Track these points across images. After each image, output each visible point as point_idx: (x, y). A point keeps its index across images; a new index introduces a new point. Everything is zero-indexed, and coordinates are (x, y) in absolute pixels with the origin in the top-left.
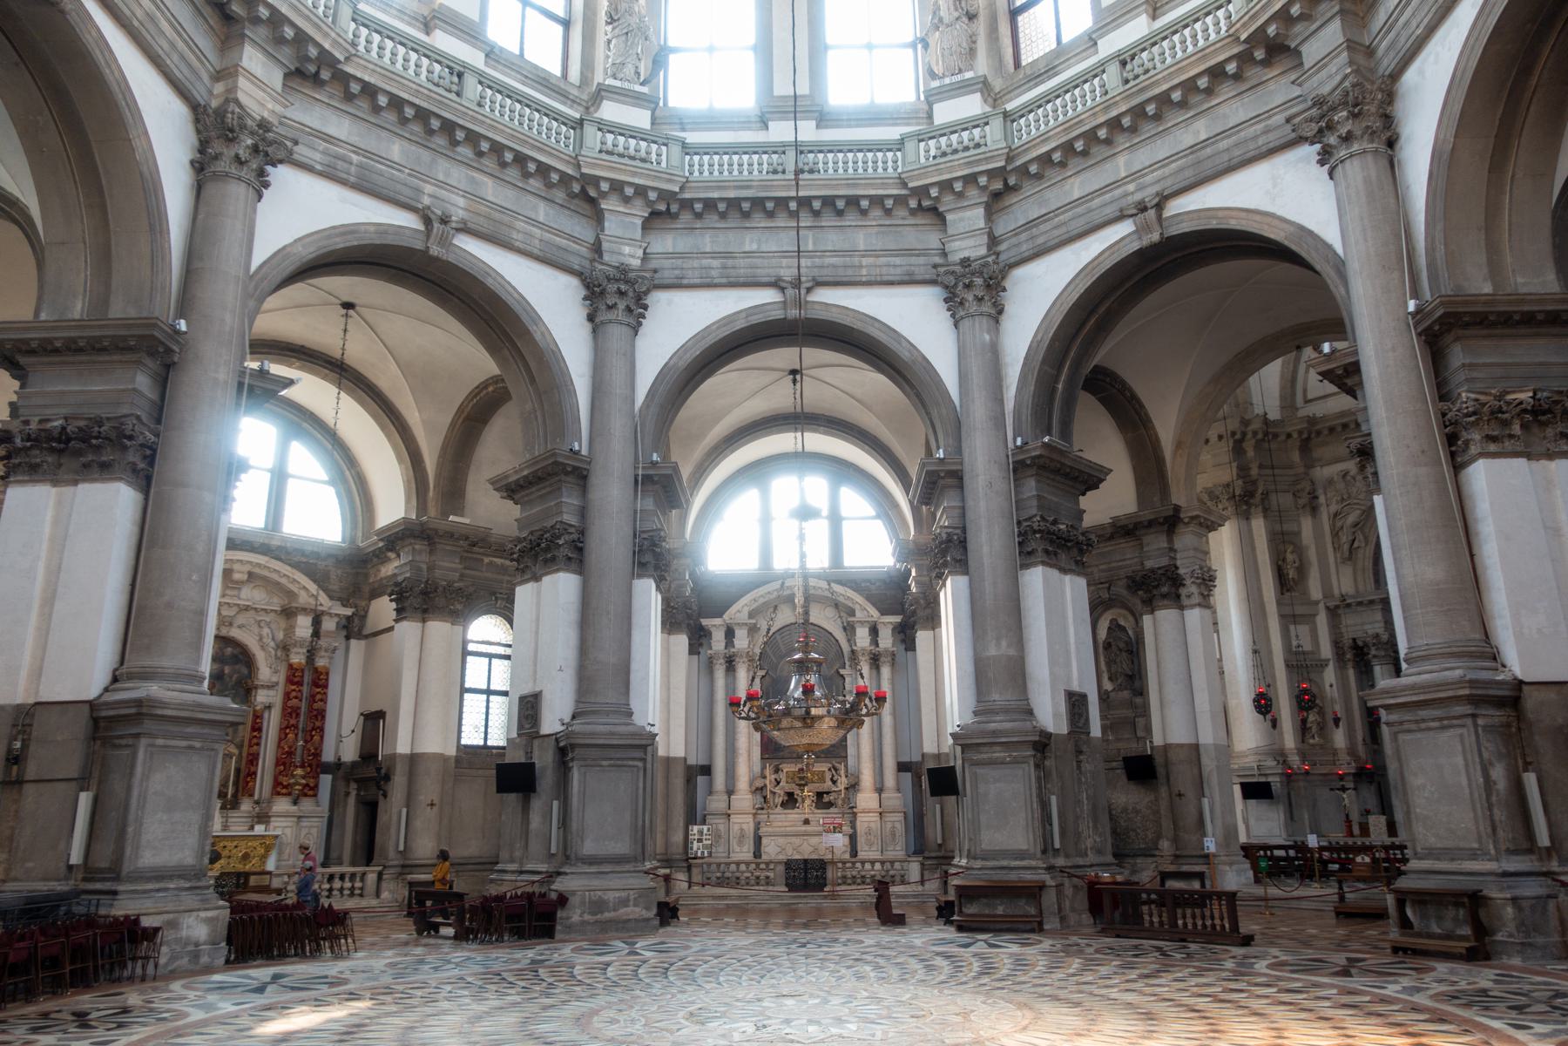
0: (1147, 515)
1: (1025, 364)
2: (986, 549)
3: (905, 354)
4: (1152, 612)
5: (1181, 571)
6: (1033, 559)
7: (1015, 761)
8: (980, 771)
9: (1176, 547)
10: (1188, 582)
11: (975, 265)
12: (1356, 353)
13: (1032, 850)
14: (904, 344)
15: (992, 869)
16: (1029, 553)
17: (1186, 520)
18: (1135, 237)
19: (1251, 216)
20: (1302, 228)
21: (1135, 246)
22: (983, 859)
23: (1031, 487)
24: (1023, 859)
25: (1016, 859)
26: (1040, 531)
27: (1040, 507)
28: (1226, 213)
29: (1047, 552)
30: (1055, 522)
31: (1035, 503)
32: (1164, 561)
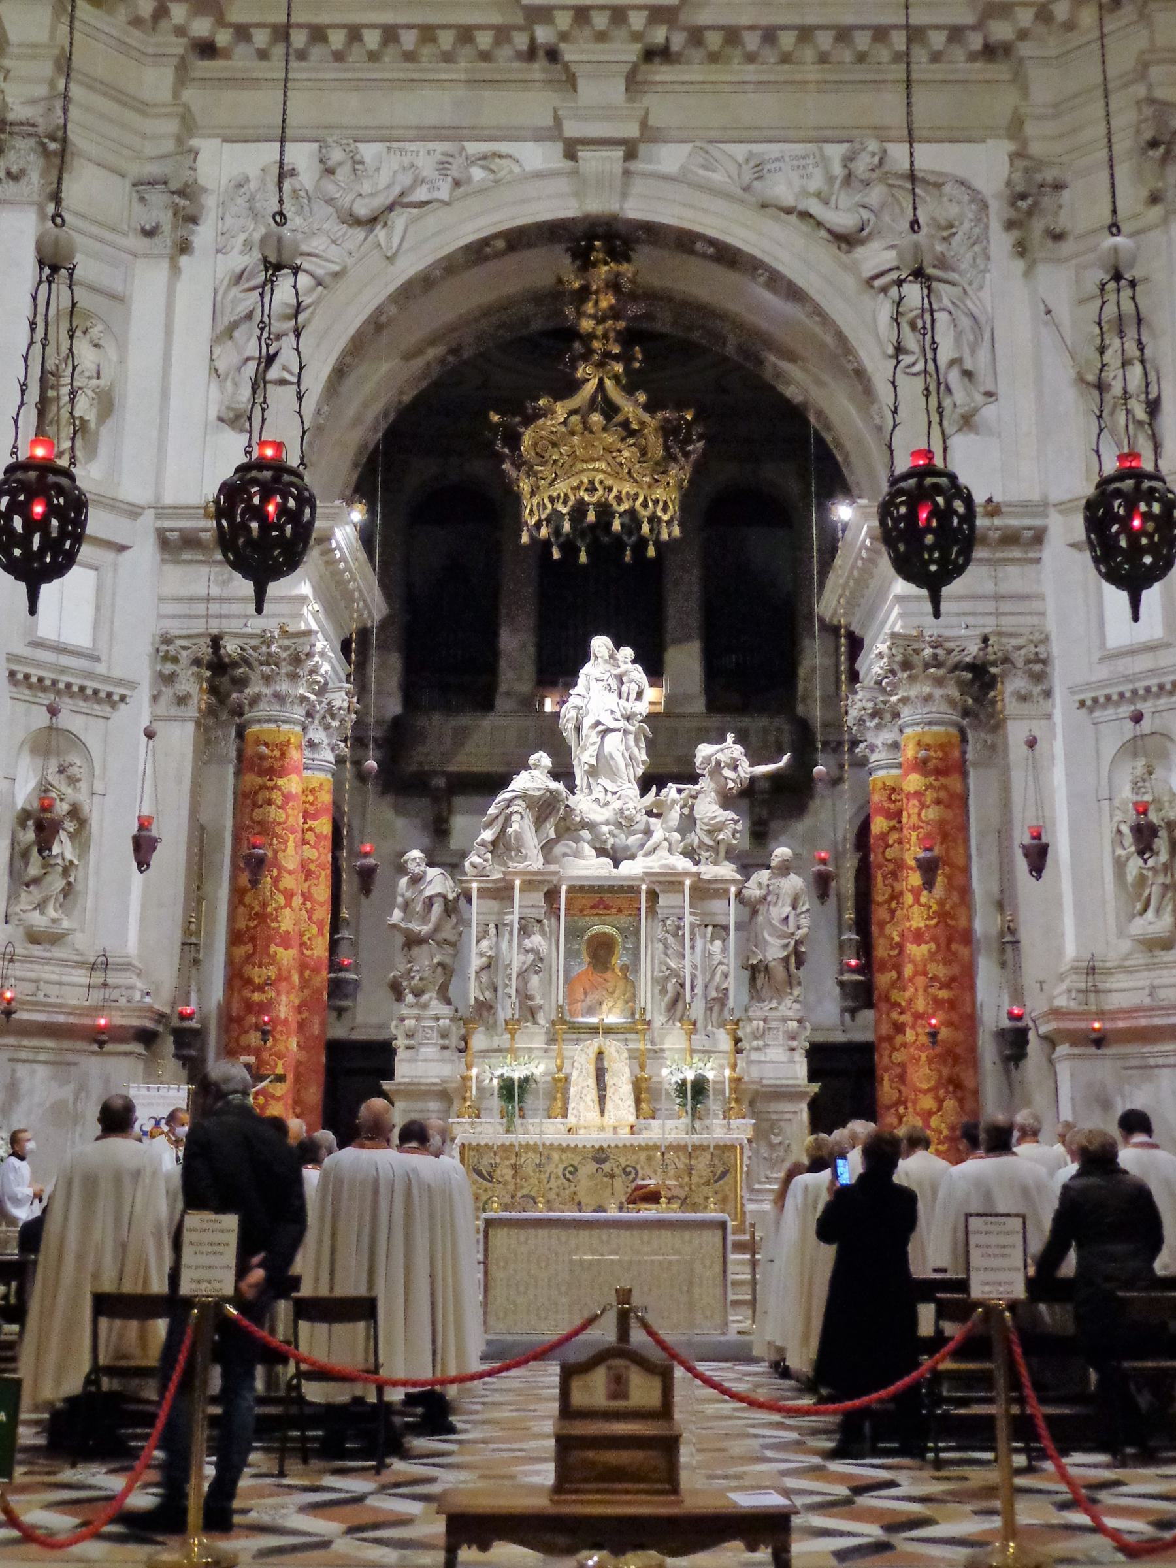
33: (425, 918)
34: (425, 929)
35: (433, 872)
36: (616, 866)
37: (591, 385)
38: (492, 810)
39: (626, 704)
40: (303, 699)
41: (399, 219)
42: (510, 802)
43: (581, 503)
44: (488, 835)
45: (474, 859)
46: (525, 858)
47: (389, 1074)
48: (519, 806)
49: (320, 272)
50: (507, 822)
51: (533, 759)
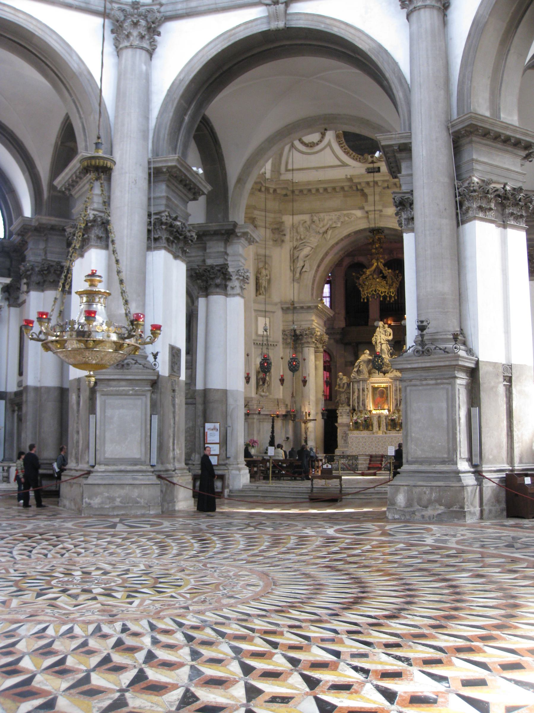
0: (214, 226)
1: (168, 95)
2: (125, 232)
3: (74, 65)
4: (207, 296)
5: (230, 270)
6: (158, 244)
7: (136, 394)
8: (111, 401)
9: (228, 252)
10: (234, 278)
11: (142, 10)
12: (410, 137)
13: (143, 459)
14: (75, 58)
15: (113, 472)
16: (156, 240)
17: (239, 234)
18: (265, 20)
19: (348, 29)
20: (380, 46)
21: (264, 28)
22: (106, 465)
23: (162, 190)
24: (136, 465)
25: (131, 465)
26: (166, 224)
27: (167, 206)
28: (332, 22)
29: (168, 240)
30: (176, 219)
31: (164, 202)
32: (220, 261)
33: (343, 388)
34: (343, 390)
35: (345, 377)
36: (384, 374)
37: (375, 264)
38: (356, 364)
39: (387, 337)
40: (314, 342)
41: (330, 232)
42: (360, 362)
43: (373, 294)
44: (355, 369)
45: (353, 375)
46: (364, 374)
47: (337, 422)
48: (362, 363)
49: (312, 246)
50: (359, 367)
51: (365, 351)
